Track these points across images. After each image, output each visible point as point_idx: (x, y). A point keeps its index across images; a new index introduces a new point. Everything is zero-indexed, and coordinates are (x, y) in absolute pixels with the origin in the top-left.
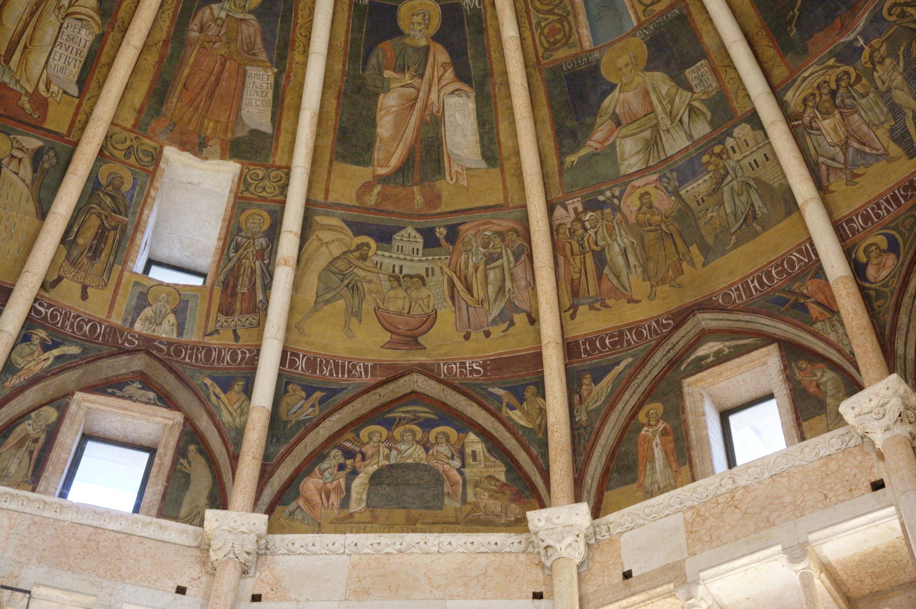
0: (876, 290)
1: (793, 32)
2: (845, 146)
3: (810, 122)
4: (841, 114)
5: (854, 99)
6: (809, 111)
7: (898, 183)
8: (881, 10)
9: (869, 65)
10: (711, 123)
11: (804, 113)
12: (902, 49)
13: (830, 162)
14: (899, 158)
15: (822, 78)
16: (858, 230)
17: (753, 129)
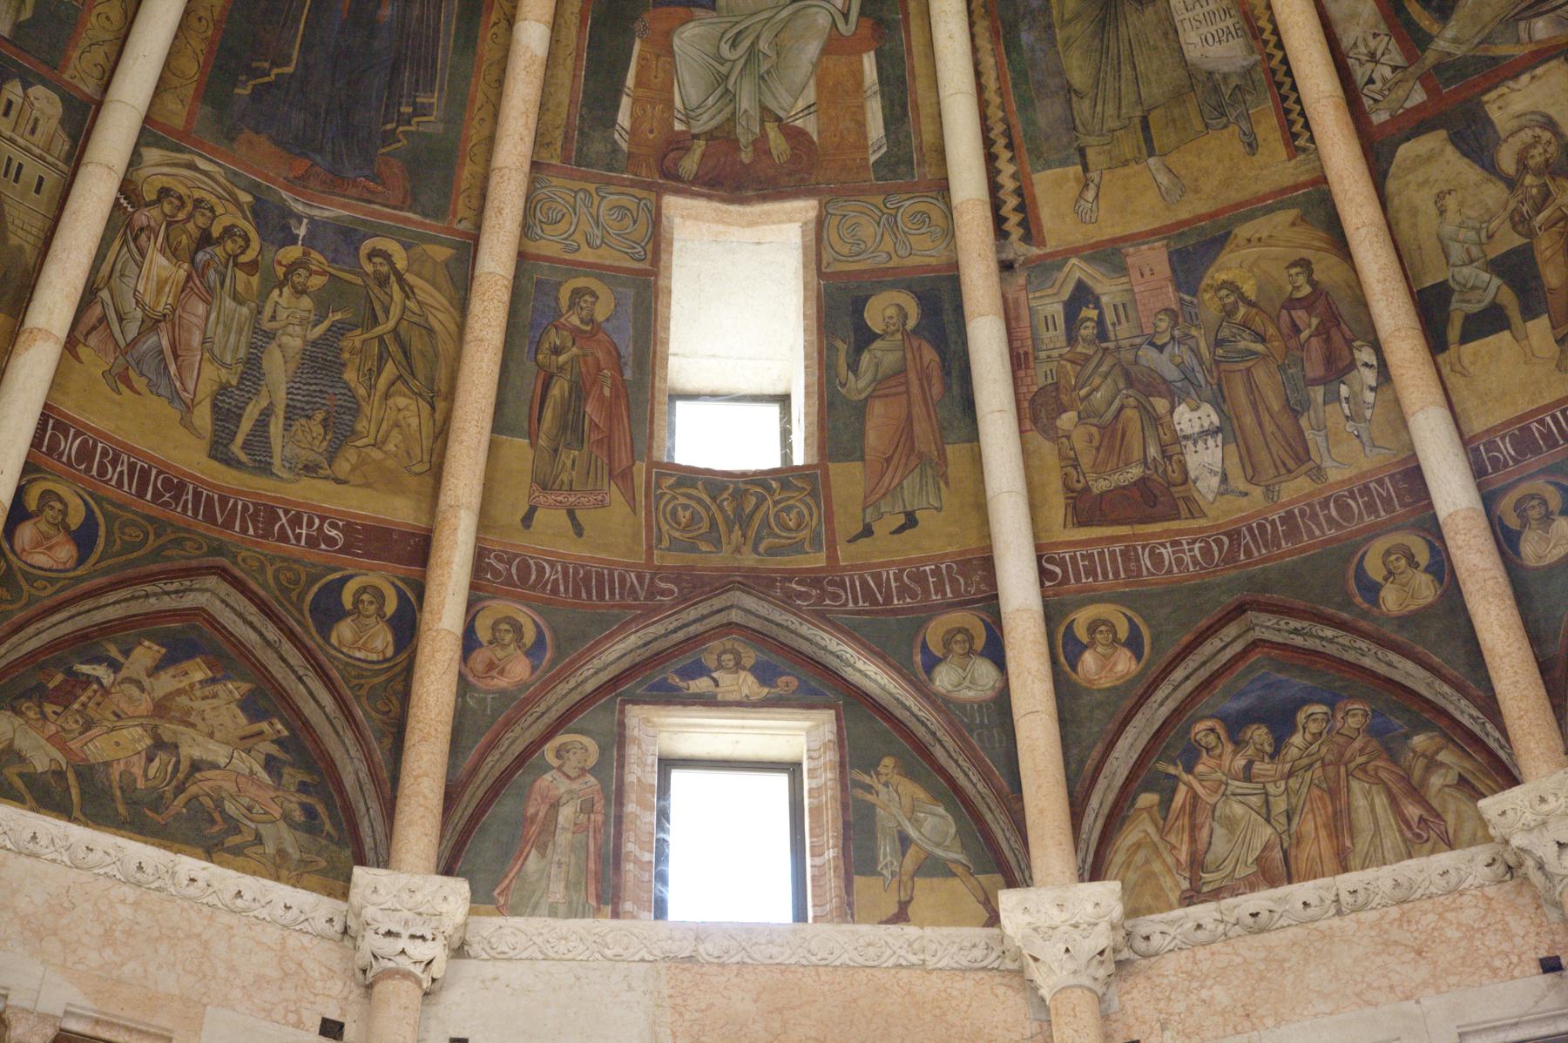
0: (10, 567)
1: (244, 91)
2: (152, 323)
3: (142, 229)
4: (189, 277)
5: (222, 284)
6: (155, 212)
7: (169, 466)
8: (366, 237)
9: (280, 271)
10: (18, 26)
11: (148, 205)
12: (338, 316)
13: (112, 316)
14: (200, 436)
15: (214, 200)
16: (61, 454)
17: (62, 122)
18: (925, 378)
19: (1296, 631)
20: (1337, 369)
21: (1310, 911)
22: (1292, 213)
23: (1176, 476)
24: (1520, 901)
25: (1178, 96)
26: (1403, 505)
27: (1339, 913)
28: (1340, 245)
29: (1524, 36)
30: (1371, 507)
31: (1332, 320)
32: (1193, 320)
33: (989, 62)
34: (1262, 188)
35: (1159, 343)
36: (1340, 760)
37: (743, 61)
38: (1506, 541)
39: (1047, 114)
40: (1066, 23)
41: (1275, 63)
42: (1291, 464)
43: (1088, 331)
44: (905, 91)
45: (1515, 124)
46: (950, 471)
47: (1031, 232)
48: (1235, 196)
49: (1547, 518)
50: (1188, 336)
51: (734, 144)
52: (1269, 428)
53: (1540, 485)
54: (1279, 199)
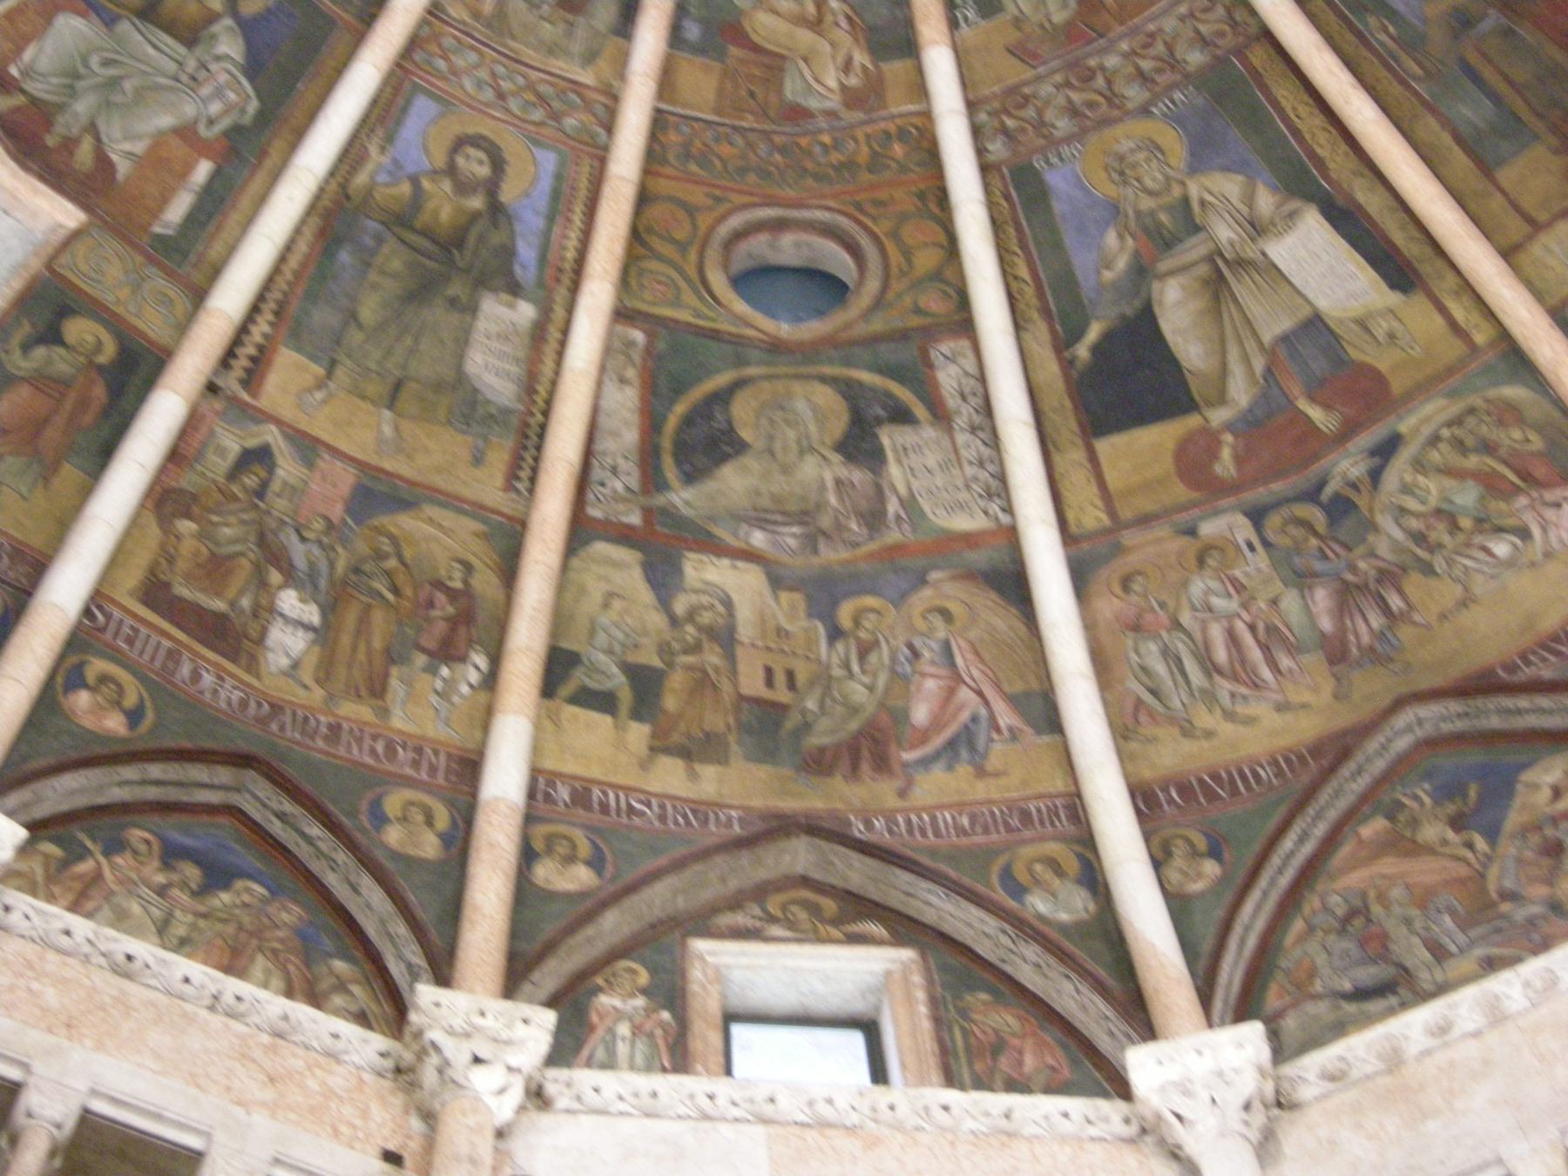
18: (83, 403)
19: (281, 816)
20: (448, 652)
21: (187, 988)
22: (478, 526)
23: (254, 634)
24: (391, 1099)
25: (439, 386)
26: (447, 779)
27: (212, 1008)
28: (509, 571)
29: (742, 534)
30: (416, 764)
31: (465, 617)
32: (344, 542)
33: (302, 247)
34: (466, 492)
35: (305, 534)
36: (258, 934)
37: (99, 80)
38: (528, 855)
39: (323, 317)
40: (383, 273)
41: (532, 421)
42: (364, 692)
43: (250, 481)
44: (222, 209)
45: (699, 585)
46: (56, 482)
47: (252, 379)
48: (439, 481)
49: (570, 859)
50: (333, 549)
51: (48, 124)
52: (361, 656)
53: (579, 835)
54: (477, 510)
